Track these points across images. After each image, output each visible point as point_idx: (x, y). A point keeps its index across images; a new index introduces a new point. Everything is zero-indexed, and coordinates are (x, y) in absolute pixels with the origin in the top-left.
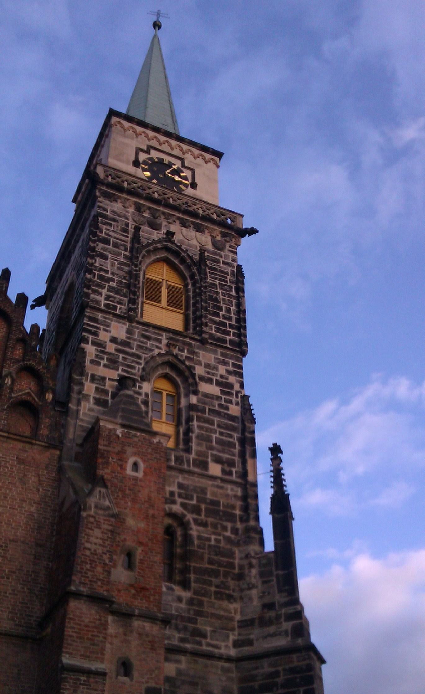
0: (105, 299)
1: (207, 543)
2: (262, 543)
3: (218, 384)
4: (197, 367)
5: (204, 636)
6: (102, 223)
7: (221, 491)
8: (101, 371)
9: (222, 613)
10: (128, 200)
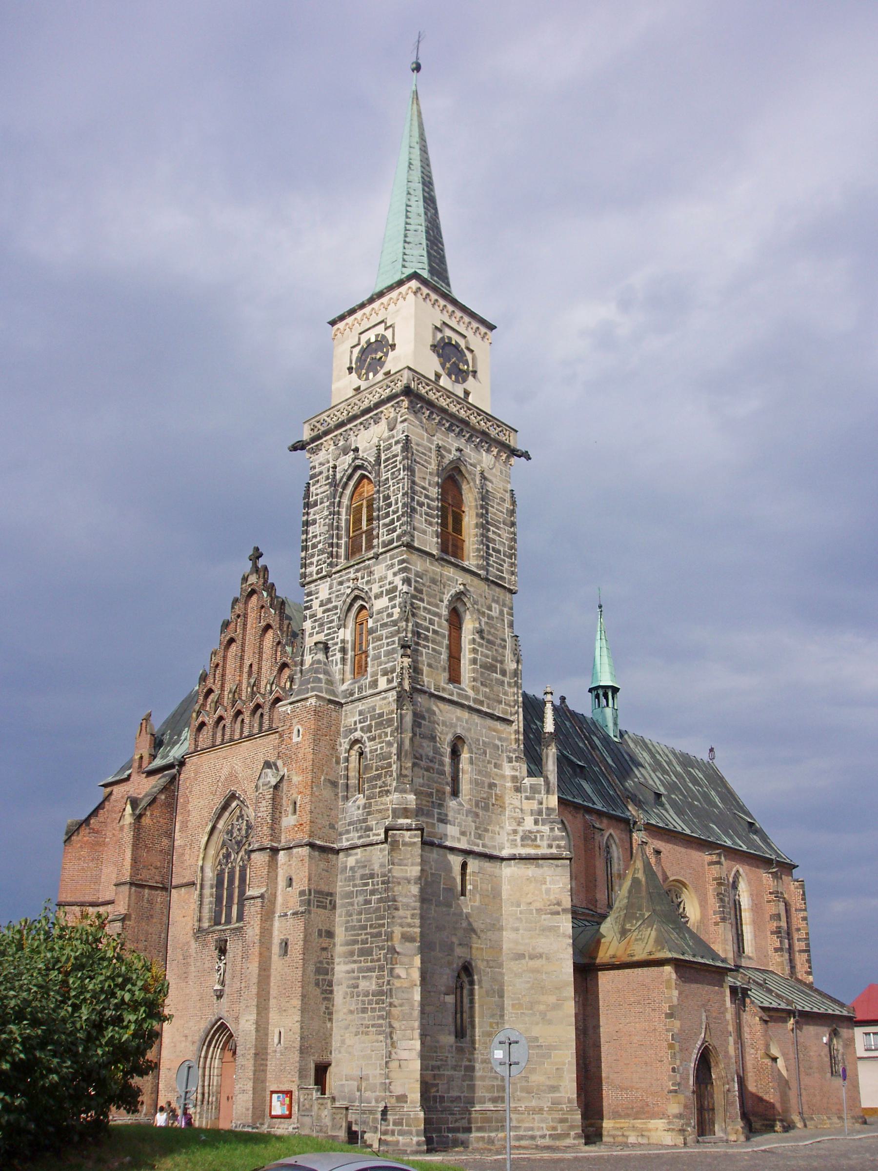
4: (373, 586)
7: (385, 702)
9: (382, 807)
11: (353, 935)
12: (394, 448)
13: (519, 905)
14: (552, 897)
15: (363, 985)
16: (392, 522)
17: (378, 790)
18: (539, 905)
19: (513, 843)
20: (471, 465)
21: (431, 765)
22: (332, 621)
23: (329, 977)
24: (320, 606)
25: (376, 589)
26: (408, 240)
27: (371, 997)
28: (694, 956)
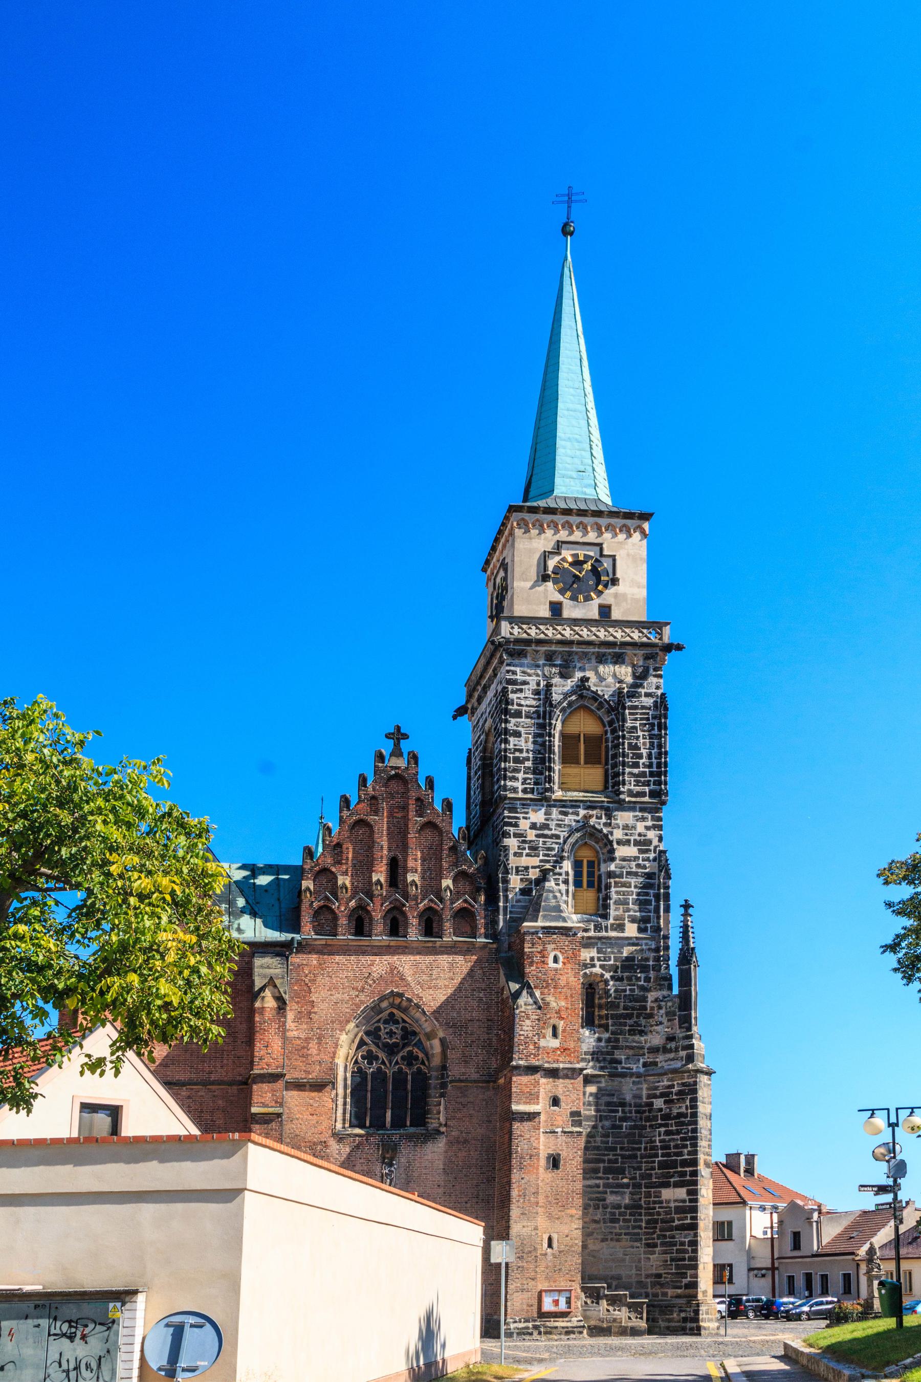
0: (523, 784)
1: (623, 994)
2: (670, 988)
3: (637, 843)
4: (615, 831)
5: (620, 1063)
6: (513, 692)
8: (525, 861)
9: (635, 1044)
10: (537, 651)
11: (596, 1155)
12: (643, 699)
15: (611, 1199)
16: (643, 774)
17: (627, 1028)
24: (530, 828)
25: (618, 834)
27: (623, 1210)
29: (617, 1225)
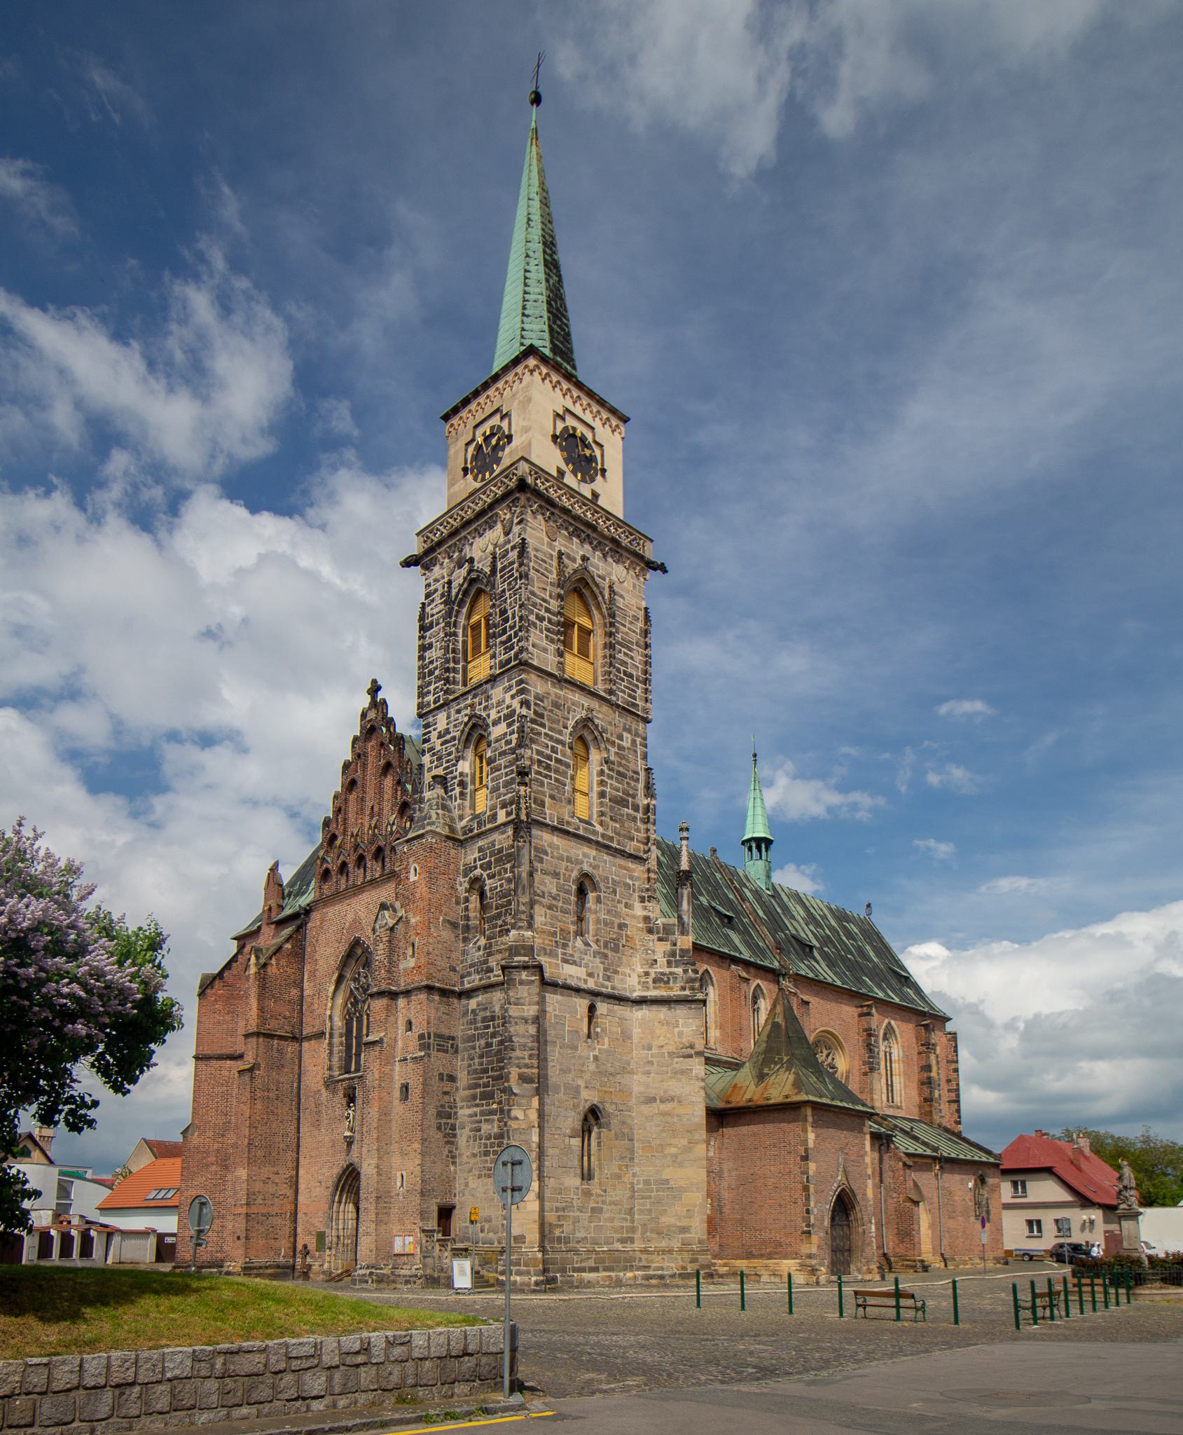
9: (503, 947)
11: (475, 1079)
13: (650, 1048)
14: (684, 1040)
15: (485, 1128)
17: (498, 929)
18: (671, 1048)
19: (645, 986)
20: (599, 576)
21: (554, 902)
22: (450, 754)
23: (452, 1121)
26: (527, 312)
27: (493, 1140)
28: (832, 1099)
29: (488, 1158)
